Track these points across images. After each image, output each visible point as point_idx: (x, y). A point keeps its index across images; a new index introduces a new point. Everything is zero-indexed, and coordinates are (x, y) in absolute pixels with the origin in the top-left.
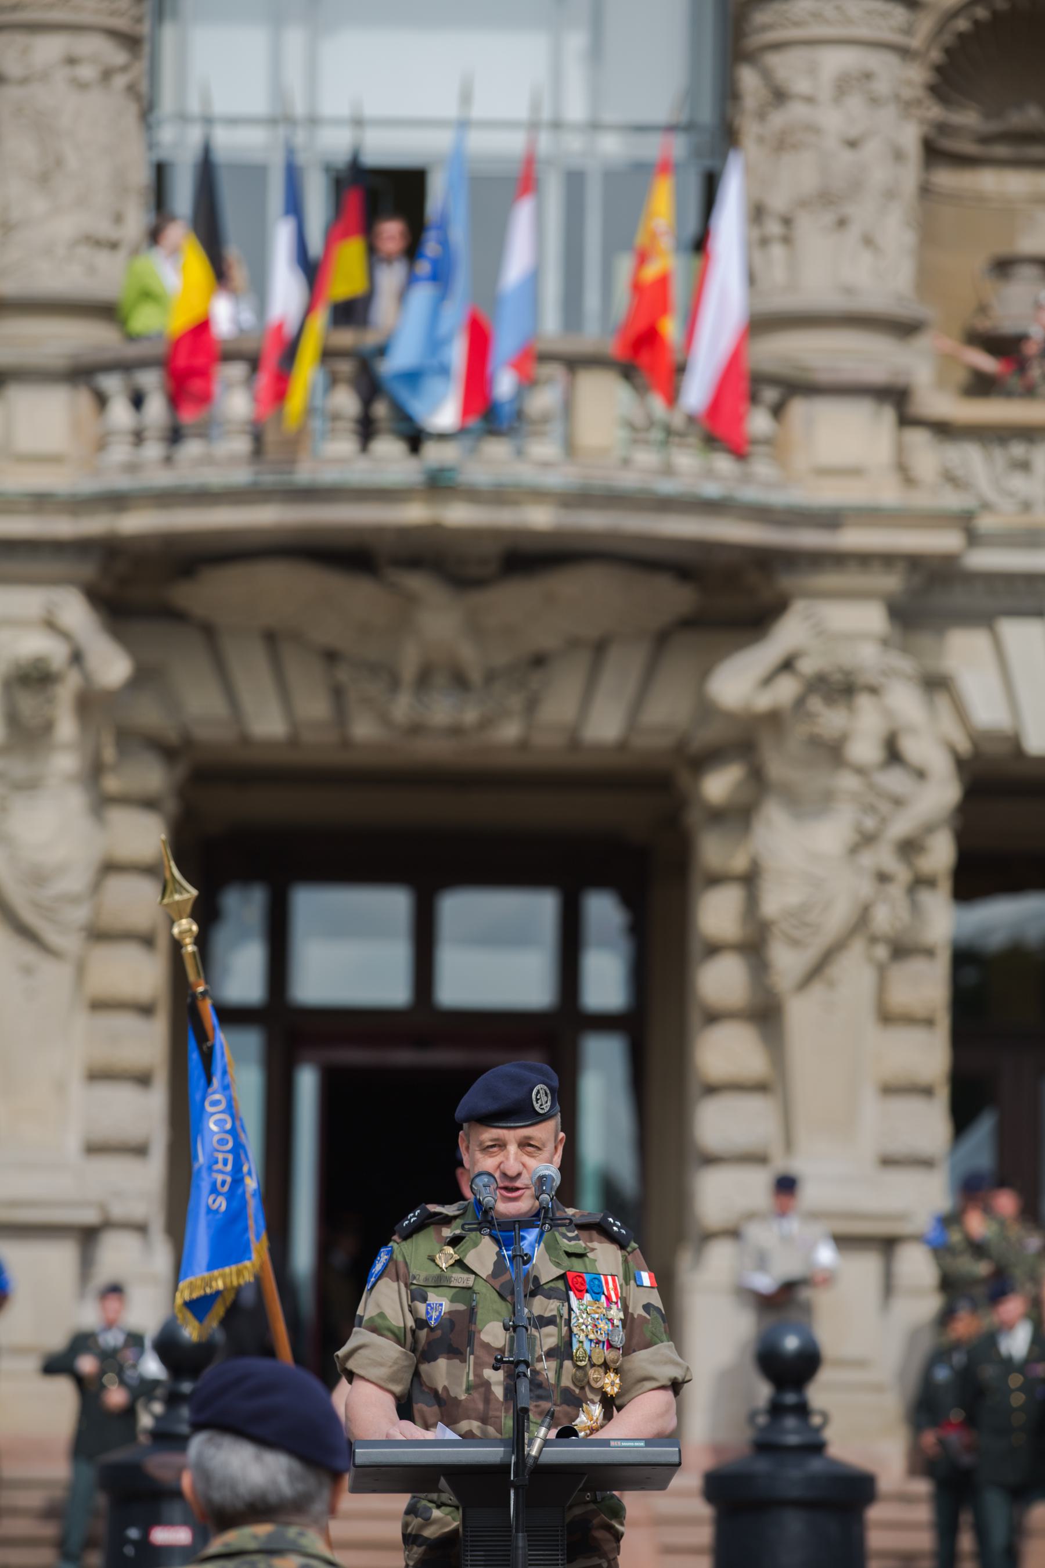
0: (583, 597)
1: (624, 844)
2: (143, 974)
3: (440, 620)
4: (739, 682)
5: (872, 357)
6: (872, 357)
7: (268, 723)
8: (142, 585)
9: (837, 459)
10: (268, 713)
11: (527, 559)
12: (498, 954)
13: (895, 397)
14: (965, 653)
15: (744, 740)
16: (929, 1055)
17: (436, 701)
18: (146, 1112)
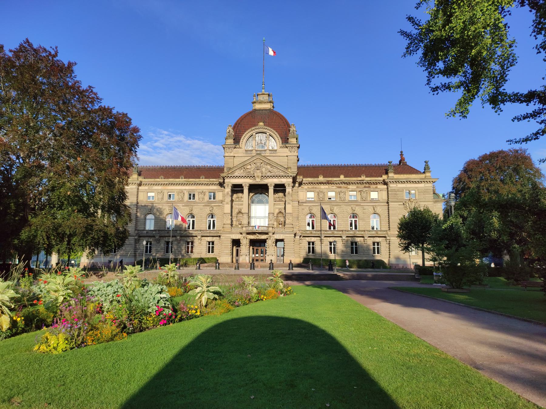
9: (271, 229)
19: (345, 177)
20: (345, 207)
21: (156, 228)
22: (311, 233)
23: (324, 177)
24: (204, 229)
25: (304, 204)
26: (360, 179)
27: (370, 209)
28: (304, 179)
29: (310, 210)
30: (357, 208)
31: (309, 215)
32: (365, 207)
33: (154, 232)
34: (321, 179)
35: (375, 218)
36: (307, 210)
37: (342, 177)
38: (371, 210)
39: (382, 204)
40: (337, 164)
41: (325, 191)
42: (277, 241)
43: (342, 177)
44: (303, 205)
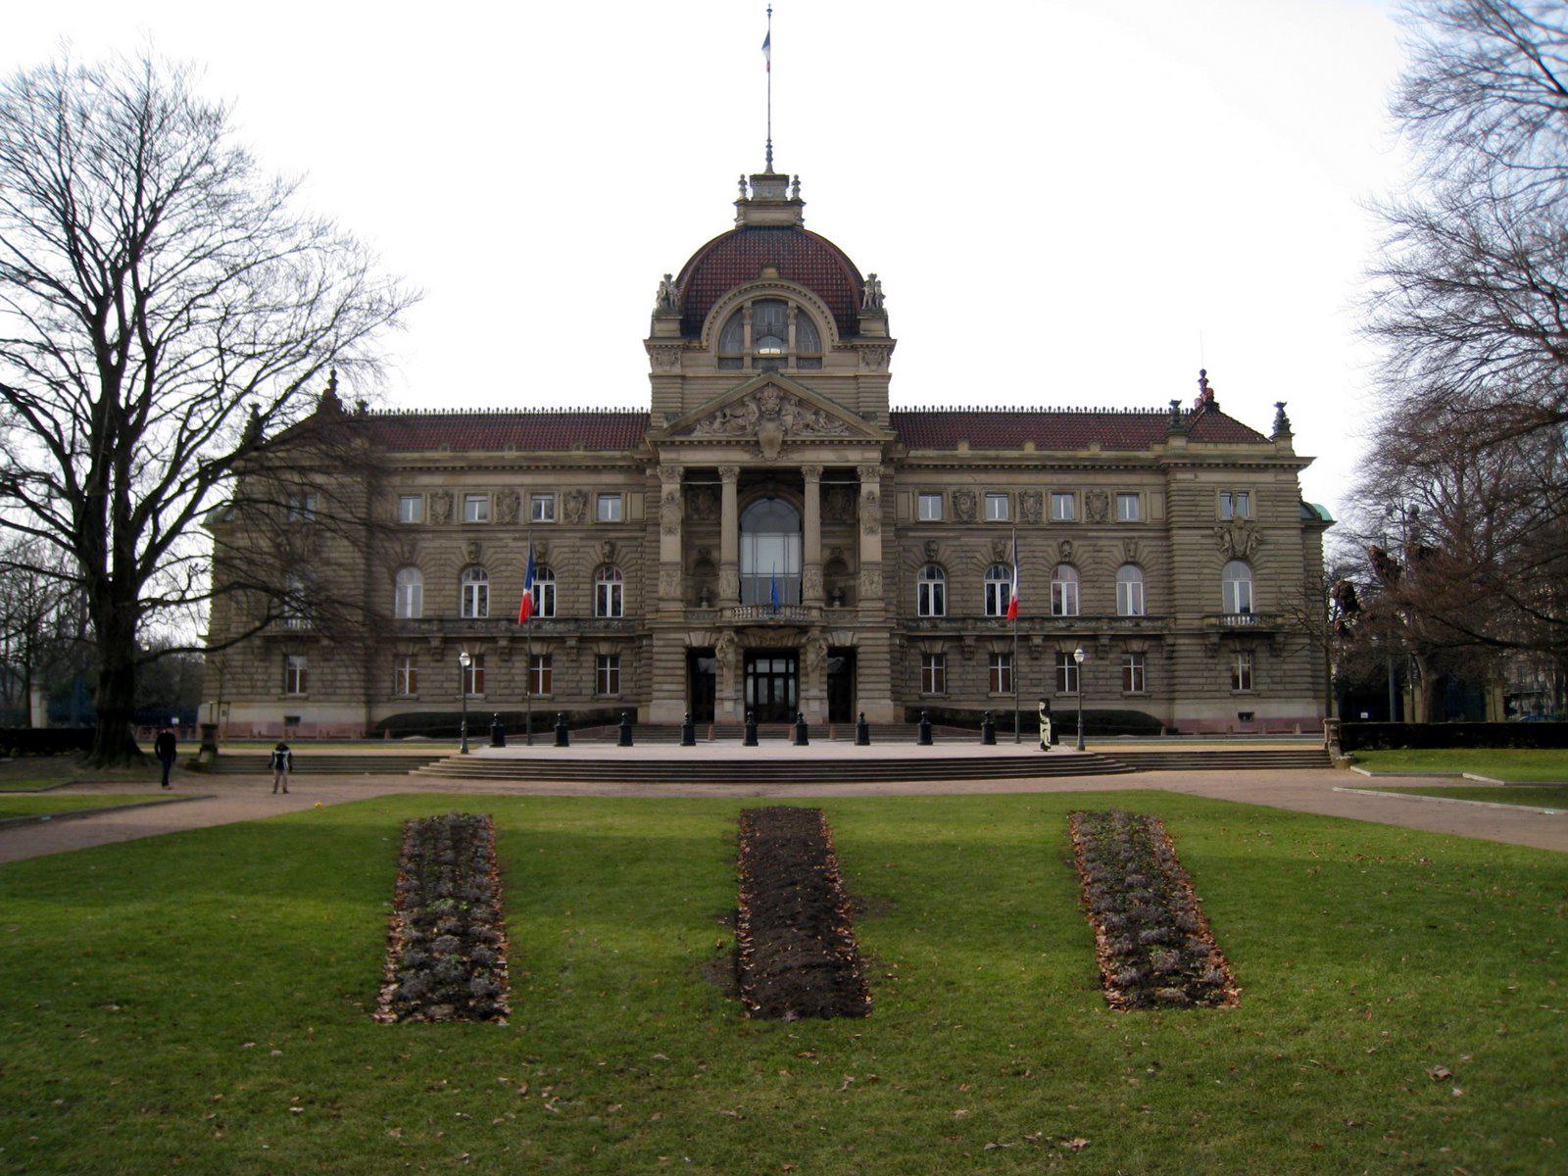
0: (786, 632)
1: (793, 655)
2: (741, 672)
3: (772, 634)
4: (804, 640)
5: (817, 604)
6: (817, 604)
7: (753, 644)
8: (740, 630)
10: (753, 643)
11: (781, 627)
12: (779, 667)
13: (821, 609)
14: (828, 636)
15: (804, 646)
16: (825, 679)
17: (770, 640)
18: (741, 687)
19: (1039, 447)
20: (1039, 542)
21: (430, 613)
22: (935, 627)
23: (972, 446)
24: (584, 613)
25: (911, 534)
26: (1083, 453)
27: (1116, 552)
28: (912, 453)
29: (928, 549)
30: (1076, 543)
31: (925, 570)
32: (1101, 543)
33: (425, 626)
34: (963, 450)
35: (1129, 579)
36: (918, 553)
37: (1030, 448)
38: (1118, 553)
39: (1151, 534)
40: (1009, 406)
41: (976, 490)
42: (834, 651)
43: (1030, 448)
44: (907, 537)
